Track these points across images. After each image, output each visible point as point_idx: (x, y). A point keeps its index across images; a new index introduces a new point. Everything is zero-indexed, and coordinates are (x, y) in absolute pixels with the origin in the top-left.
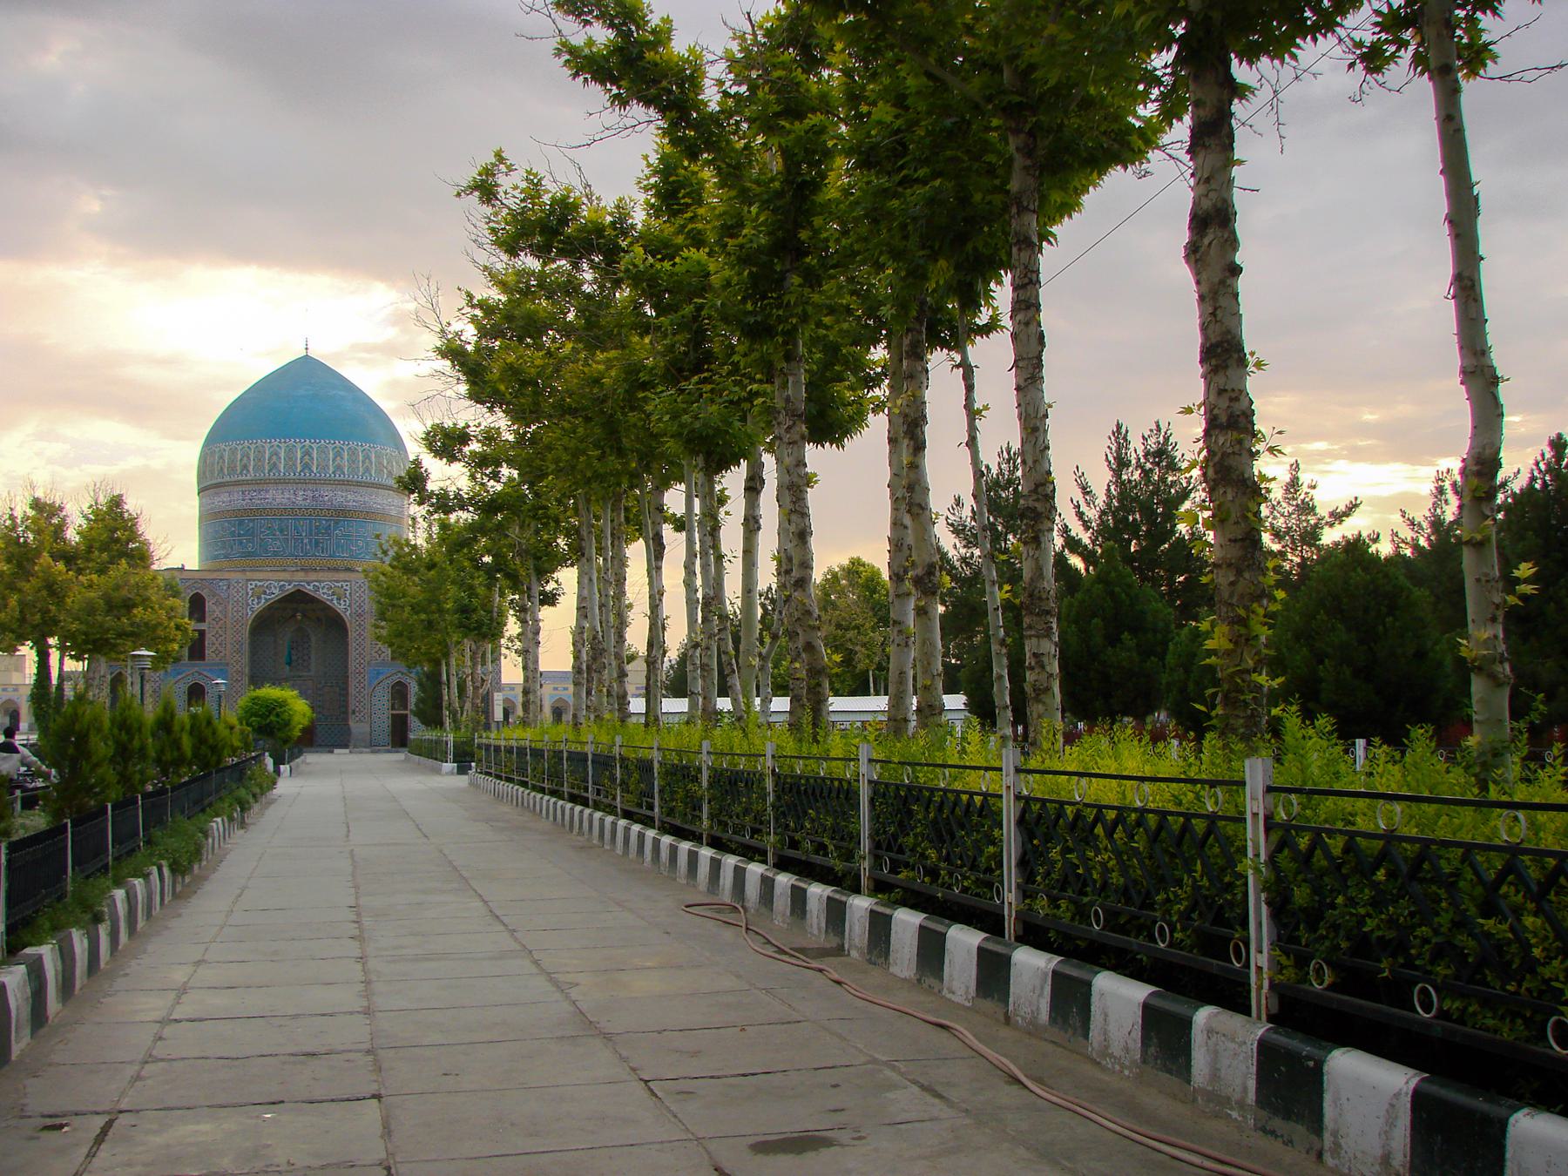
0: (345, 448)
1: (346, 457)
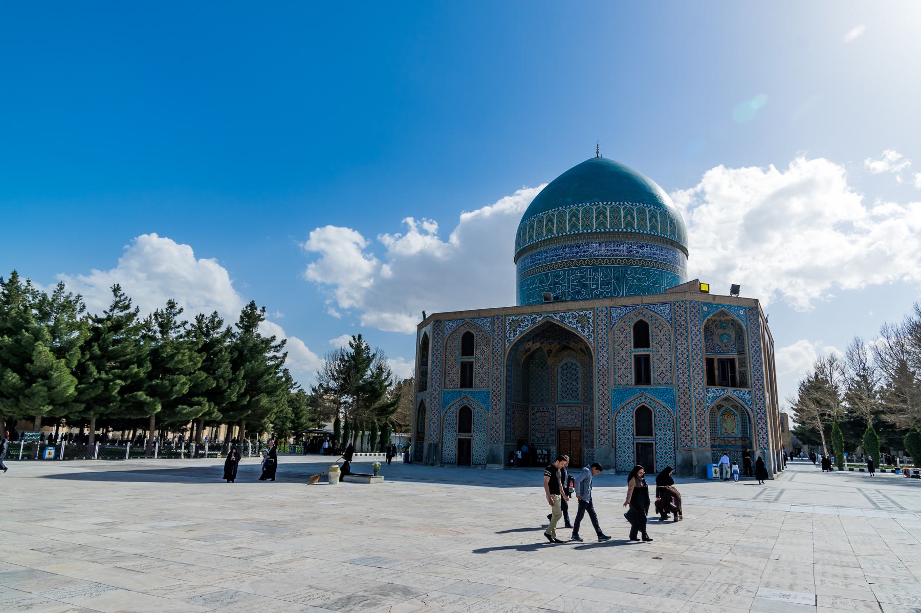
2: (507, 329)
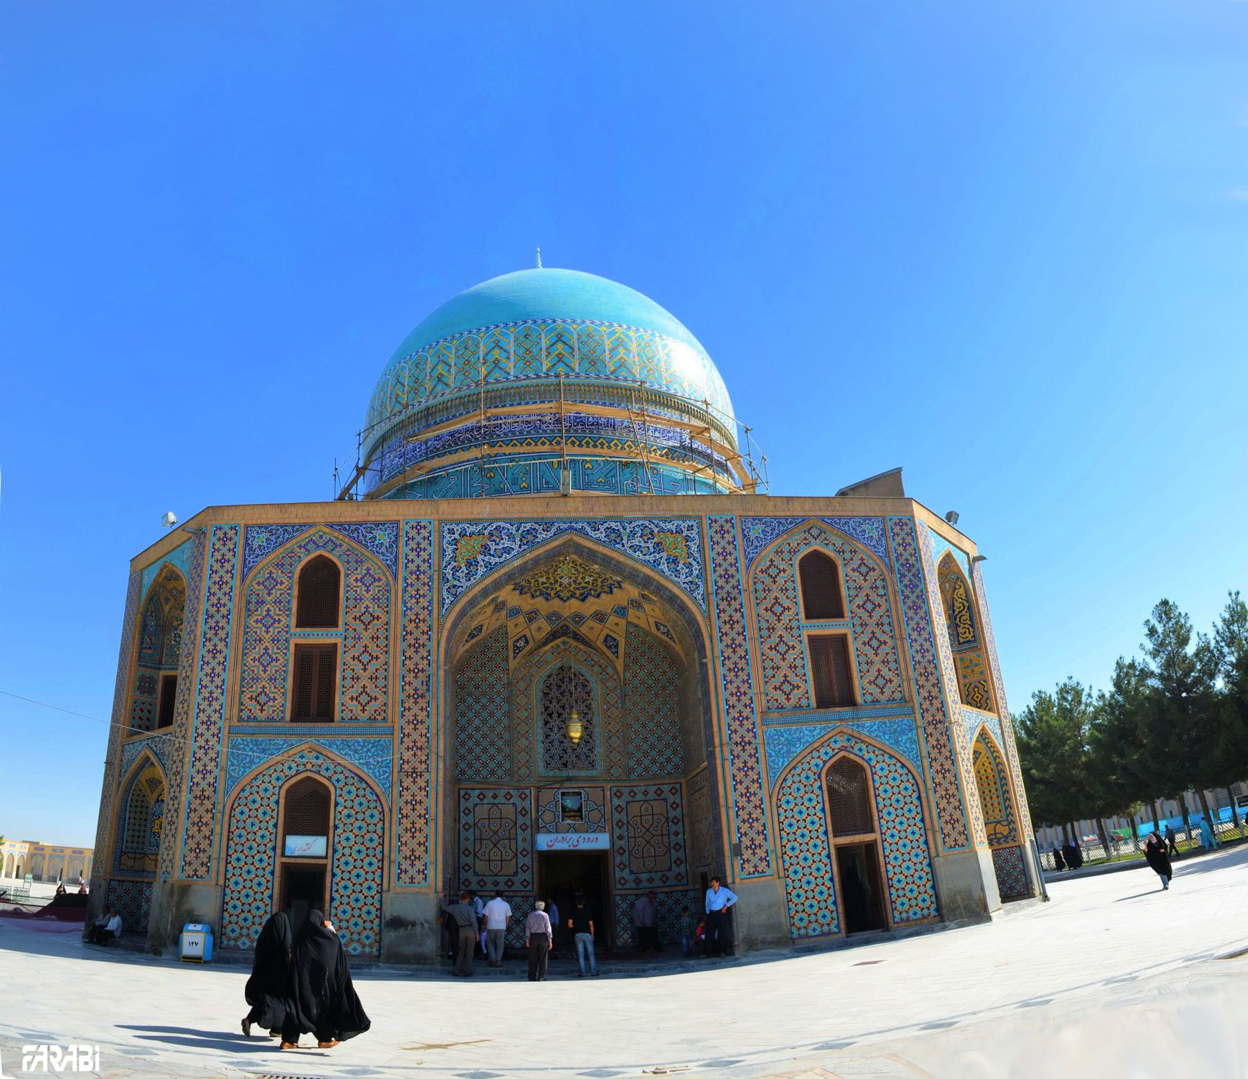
2: (447, 559)
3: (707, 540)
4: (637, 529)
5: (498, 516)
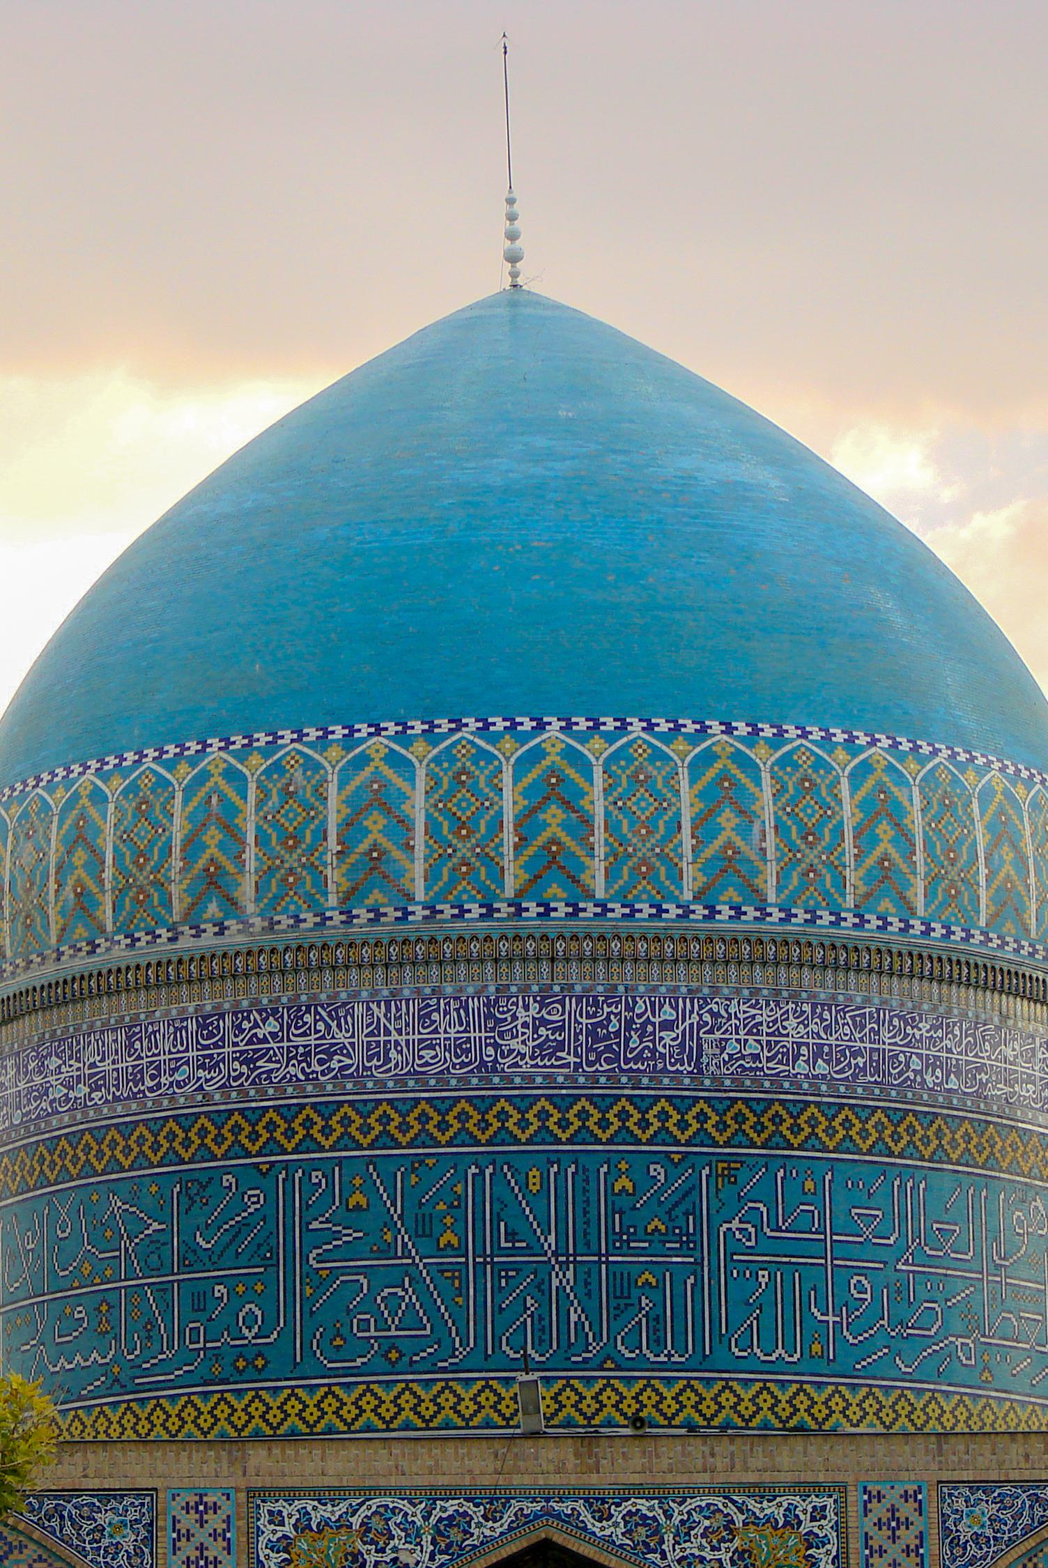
0: (761, 755)
1: (766, 805)
3: (855, 1544)
4: (696, 1517)
5: (382, 1482)
